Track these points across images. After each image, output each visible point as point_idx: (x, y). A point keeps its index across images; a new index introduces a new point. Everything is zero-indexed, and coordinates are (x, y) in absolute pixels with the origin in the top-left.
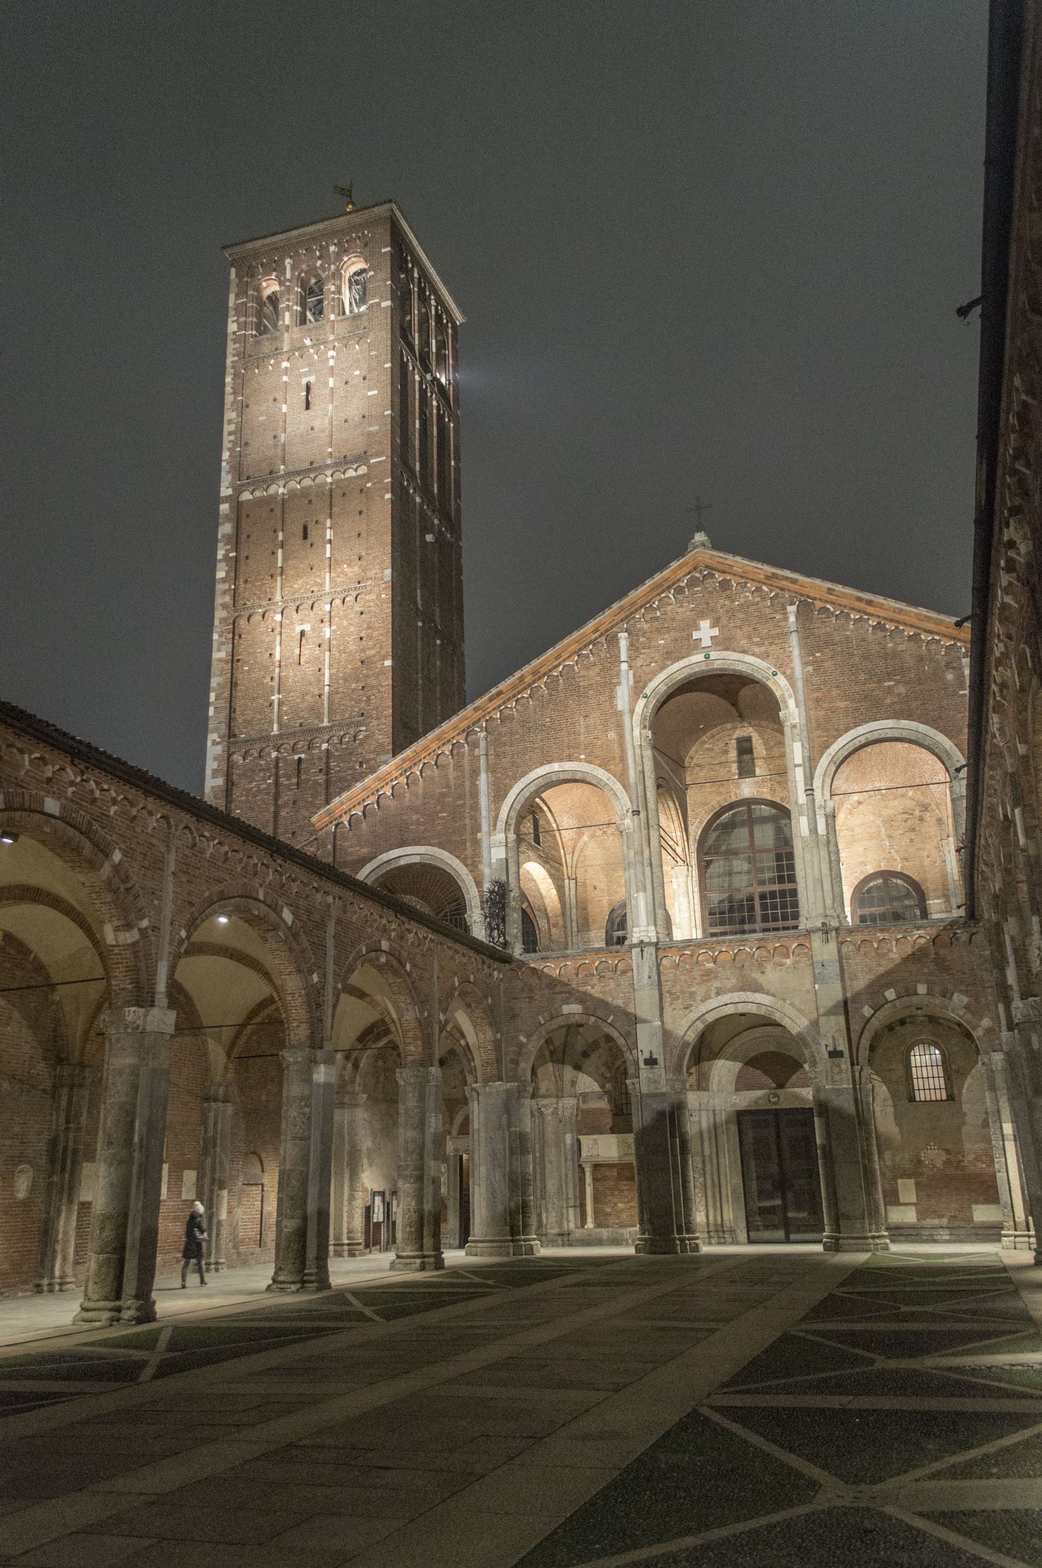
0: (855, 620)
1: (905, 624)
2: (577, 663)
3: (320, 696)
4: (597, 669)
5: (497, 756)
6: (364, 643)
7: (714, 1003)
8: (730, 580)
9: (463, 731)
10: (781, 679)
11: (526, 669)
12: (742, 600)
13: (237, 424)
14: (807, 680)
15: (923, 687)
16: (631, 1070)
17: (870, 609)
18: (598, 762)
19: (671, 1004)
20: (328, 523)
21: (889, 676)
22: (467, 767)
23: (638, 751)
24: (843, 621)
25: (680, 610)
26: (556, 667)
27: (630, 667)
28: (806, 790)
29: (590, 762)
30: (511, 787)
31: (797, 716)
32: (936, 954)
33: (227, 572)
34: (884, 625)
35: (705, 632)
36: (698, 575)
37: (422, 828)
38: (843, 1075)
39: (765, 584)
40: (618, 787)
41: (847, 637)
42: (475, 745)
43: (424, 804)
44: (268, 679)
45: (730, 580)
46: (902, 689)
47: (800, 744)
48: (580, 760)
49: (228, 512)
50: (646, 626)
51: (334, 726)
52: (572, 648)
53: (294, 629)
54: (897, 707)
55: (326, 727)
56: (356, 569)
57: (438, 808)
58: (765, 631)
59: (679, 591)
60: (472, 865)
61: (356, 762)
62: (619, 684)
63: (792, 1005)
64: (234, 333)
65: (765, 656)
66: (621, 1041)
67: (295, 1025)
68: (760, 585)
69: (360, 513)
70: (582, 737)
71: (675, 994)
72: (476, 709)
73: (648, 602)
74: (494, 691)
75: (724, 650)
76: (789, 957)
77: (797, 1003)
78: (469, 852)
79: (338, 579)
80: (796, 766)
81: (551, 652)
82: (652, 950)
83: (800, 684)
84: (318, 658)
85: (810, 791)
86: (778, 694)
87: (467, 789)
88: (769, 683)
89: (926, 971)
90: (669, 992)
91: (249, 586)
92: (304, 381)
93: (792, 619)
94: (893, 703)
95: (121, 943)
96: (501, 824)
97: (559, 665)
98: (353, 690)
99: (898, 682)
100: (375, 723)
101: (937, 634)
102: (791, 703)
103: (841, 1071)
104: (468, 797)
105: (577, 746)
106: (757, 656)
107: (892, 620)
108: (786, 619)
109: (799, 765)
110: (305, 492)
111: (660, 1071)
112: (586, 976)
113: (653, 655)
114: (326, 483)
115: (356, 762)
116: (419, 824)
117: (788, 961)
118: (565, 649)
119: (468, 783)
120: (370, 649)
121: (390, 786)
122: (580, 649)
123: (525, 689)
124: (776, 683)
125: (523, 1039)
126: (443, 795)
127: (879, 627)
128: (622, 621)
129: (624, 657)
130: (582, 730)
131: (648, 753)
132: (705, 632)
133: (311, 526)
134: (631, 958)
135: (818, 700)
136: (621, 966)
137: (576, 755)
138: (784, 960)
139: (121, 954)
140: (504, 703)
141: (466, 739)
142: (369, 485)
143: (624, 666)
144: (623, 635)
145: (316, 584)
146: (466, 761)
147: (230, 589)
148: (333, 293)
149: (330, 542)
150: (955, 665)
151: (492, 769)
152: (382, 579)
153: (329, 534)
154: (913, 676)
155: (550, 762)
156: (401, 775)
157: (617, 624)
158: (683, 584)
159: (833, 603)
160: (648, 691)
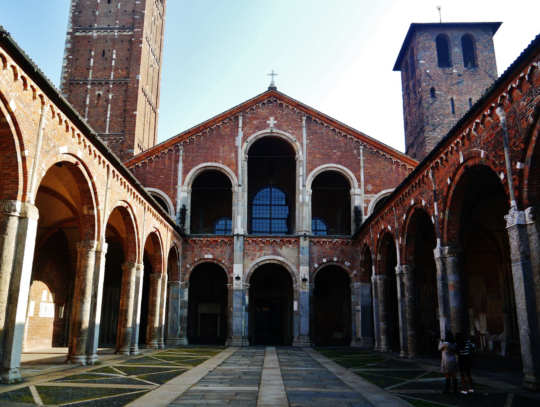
0: (326, 127)
1: (342, 130)
2: (222, 125)
3: (105, 121)
5: (186, 156)
7: (262, 259)
8: (282, 104)
9: (174, 145)
10: (298, 144)
12: (286, 112)
13: (77, 3)
14: (307, 145)
15: (346, 154)
16: (229, 281)
17: (331, 123)
18: (226, 164)
19: (247, 258)
20: (115, 51)
21: (335, 148)
22: (173, 159)
23: (243, 162)
24: (321, 126)
25: (263, 111)
26: (213, 125)
27: (242, 130)
28: (303, 185)
29: (223, 164)
30: (191, 170)
31: (302, 158)
32: (341, 248)
33: (67, 64)
34: (335, 130)
35: (272, 121)
36: (271, 100)
37: (153, 181)
38: (306, 287)
39: (295, 107)
40: (233, 175)
41: (322, 132)
42: (178, 151)
43: (154, 171)
44: (82, 112)
45: (283, 104)
46: (339, 154)
47: (302, 168)
48: (220, 163)
49: (70, 39)
50: (250, 116)
51: (110, 134)
53: (95, 93)
54: (337, 160)
55: (107, 135)
56: (124, 73)
58: (294, 125)
59: (264, 104)
60: (172, 198)
61: (118, 150)
62: (237, 136)
63: (291, 262)
65: (293, 134)
66: (226, 270)
67: (130, 253)
68: (293, 107)
69: (128, 50)
70: (221, 154)
71: (249, 254)
73: (251, 106)
75: (278, 129)
76: (291, 244)
77: (292, 261)
78: (172, 192)
79: (116, 75)
80: (300, 176)
82: (243, 237)
83: (305, 147)
84: (105, 106)
85: (304, 186)
86: (296, 149)
87: (173, 168)
88: (293, 144)
89: (337, 253)
90: (246, 253)
93: (304, 122)
94: (336, 158)
95: (90, 214)
96: (186, 183)
97: (215, 124)
98: (119, 121)
99: (338, 151)
101: (353, 136)
102: (301, 153)
103: (306, 285)
105: (219, 157)
106: (290, 133)
107: (338, 128)
108: (302, 121)
109: (301, 176)
110: (105, 37)
111: (241, 281)
112: (215, 244)
113: (251, 127)
114: (115, 35)
115: (118, 150)
116: (152, 179)
117: (291, 246)
120: (128, 106)
121: (140, 162)
122: (223, 120)
123: (200, 132)
124: (295, 144)
125: (188, 266)
126: (163, 169)
127: (334, 130)
128: (241, 111)
129: (240, 125)
130: (221, 151)
131: (246, 163)
132: (272, 121)
134: (233, 240)
135: (310, 153)
136: (229, 242)
137: (218, 160)
138: (289, 245)
139: (89, 219)
140: (191, 136)
141: (174, 148)
142: (133, 39)
143: (240, 129)
144: (241, 118)
145: (107, 76)
146: (173, 156)
147: (68, 71)
150: (357, 148)
151: (184, 162)
152: (135, 78)
154: (343, 149)
155: (207, 162)
156: (146, 158)
157: (239, 112)
158: (265, 102)
159: (318, 119)
160: (248, 140)
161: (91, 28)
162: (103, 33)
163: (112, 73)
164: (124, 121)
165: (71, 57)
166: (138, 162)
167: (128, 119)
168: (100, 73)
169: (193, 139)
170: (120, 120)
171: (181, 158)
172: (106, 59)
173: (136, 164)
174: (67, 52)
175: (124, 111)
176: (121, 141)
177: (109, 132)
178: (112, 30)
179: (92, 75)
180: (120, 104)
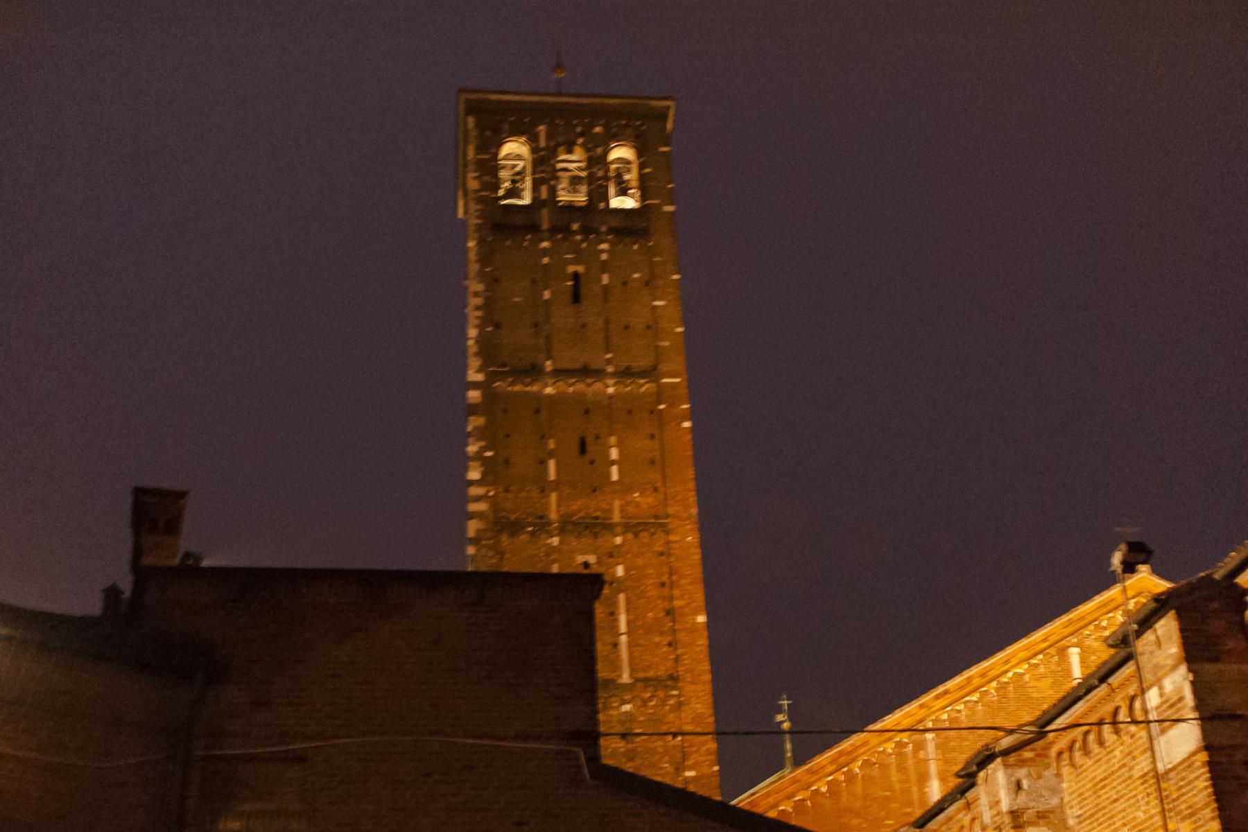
3: (615, 645)
4: (1051, 680)
6: (666, 591)
11: (974, 670)
26: (1006, 672)
33: (484, 474)
52: (1022, 655)
56: (650, 500)
57: (883, 813)
64: (476, 191)
69: (652, 437)
72: (921, 706)
74: (941, 689)
81: (1000, 656)
91: (511, 495)
92: (571, 269)
98: (658, 645)
100: (690, 688)
104: (916, 805)
118: (1013, 655)
119: (915, 789)
126: (887, 799)
128: (1071, 634)
133: (590, 439)
140: (951, 704)
148: (599, 179)
149: (613, 463)
153: (614, 454)
156: (836, 771)
161: (534, 371)
162: (572, 388)
163: (617, 504)
164: (670, 644)
165: (489, 454)
166: (815, 781)
167: (682, 637)
168: (580, 503)
169: (959, 711)
170: (657, 639)
171: (933, 768)
172: (592, 463)
173: (810, 786)
174: (479, 439)
175: (668, 613)
176: (672, 702)
177: (631, 676)
178: (598, 374)
179: (559, 505)
180: (653, 593)
